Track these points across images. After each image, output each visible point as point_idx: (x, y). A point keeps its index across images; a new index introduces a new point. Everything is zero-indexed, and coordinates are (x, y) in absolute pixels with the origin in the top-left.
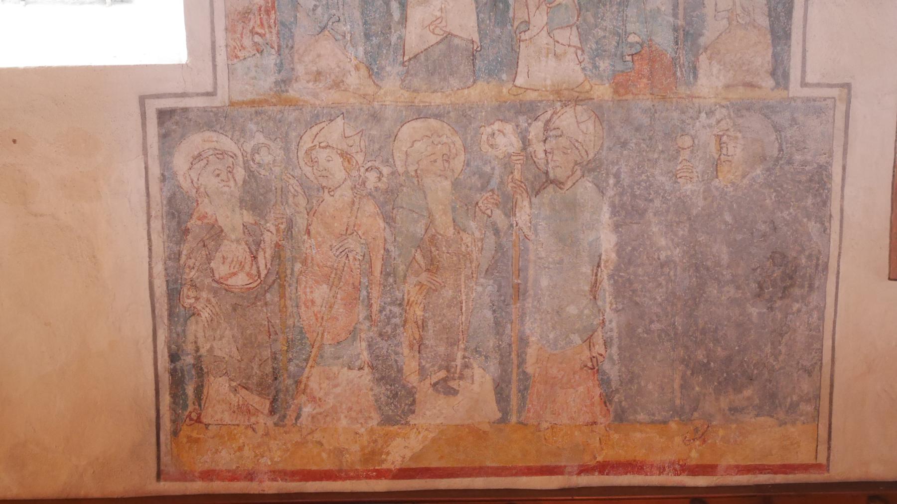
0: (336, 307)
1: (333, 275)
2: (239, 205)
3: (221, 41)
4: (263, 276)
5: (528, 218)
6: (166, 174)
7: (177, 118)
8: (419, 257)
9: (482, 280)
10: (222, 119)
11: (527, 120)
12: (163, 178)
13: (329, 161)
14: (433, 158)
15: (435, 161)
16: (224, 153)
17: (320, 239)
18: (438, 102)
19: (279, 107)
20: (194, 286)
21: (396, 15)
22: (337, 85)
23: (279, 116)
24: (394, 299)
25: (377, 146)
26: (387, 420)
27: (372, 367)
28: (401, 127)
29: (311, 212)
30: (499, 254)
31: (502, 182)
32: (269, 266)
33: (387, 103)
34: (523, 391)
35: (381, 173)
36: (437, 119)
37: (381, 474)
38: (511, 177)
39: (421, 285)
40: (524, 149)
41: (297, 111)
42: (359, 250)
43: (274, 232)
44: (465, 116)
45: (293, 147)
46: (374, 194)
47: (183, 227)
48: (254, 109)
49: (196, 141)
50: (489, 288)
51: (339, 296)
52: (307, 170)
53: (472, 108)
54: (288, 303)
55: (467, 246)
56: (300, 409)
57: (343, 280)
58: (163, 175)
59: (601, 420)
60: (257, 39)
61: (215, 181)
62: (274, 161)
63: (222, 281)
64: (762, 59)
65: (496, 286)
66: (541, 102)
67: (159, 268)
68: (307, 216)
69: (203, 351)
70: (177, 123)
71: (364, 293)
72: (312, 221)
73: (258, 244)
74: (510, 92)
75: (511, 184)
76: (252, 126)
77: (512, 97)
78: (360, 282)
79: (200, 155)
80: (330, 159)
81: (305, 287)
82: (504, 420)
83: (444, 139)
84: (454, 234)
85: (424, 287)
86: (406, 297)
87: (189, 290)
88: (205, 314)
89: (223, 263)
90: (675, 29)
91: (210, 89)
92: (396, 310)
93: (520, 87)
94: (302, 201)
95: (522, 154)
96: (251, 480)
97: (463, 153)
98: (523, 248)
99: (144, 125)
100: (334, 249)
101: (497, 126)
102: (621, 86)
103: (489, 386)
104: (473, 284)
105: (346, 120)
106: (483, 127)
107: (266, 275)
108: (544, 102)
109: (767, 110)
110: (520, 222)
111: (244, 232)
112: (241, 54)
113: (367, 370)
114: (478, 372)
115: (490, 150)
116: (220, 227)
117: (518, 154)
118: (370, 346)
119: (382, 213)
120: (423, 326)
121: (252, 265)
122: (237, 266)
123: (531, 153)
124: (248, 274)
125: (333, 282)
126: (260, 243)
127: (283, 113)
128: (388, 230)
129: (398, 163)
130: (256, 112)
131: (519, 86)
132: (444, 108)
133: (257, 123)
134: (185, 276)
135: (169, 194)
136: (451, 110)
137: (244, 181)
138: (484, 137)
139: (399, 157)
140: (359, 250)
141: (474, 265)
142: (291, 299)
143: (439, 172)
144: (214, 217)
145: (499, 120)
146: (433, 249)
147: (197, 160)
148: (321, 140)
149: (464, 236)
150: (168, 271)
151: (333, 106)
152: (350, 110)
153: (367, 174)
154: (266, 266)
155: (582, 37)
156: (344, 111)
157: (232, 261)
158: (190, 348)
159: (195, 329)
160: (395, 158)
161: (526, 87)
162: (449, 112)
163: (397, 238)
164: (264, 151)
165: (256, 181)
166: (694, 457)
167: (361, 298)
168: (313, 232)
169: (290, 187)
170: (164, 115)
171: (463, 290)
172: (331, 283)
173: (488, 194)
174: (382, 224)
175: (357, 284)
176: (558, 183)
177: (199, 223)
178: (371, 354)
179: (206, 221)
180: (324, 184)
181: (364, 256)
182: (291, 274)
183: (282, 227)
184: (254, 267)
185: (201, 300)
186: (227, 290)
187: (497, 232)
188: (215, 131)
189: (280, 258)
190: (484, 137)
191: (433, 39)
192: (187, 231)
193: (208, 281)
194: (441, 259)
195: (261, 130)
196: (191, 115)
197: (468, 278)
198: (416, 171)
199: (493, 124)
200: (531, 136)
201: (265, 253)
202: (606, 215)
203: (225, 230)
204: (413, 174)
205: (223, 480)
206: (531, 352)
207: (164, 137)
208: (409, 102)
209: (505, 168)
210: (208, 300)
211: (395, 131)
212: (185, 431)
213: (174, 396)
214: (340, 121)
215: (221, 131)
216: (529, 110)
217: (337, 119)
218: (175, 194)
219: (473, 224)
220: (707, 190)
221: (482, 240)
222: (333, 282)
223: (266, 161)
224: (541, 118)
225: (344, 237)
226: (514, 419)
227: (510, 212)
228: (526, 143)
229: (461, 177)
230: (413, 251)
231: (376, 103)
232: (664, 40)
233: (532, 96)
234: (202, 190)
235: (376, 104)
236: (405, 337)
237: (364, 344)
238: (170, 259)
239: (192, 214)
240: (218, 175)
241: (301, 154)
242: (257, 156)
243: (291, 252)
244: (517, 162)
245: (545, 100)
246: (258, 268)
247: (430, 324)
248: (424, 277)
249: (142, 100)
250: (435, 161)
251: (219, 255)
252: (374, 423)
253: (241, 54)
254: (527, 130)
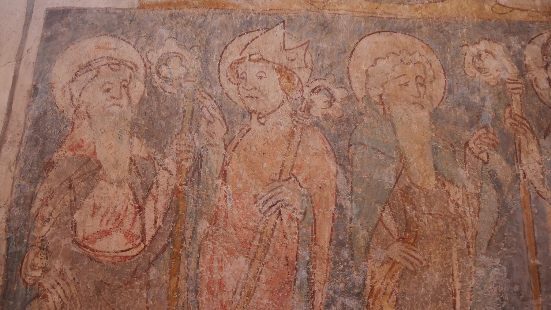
0: (258, 295)
1: (256, 243)
2: (129, 130)
4: (148, 238)
5: (538, 167)
6: (39, 86)
7: (70, 19)
8: (387, 218)
9: (483, 258)
10: (127, 23)
11: (520, 42)
12: (34, 91)
13: (261, 78)
14: (403, 80)
15: (406, 84)
16: (120, 63)
17: (240, 185)
18: (406, 15)
19: (201, 10)
20: (44, 249)
23: (200, 21)
24: (350, 285)
25: (327, 62)
28: (360, 41)
30: (505, 218)
31: (496, 117)
32: (159, 223)
33: (340, 12)
35: (332, 96)
36: (405, 34)
38: (508, 110)
39: (391, 262)
40: (522, 75)
41: (223, 15)
42: (297, 204)
43: (174, 172)
44: (442, 32)
45: (214, 58)
46: (323, 123)
47: (46, 160)
48: (169, 11)
50: (495, 271)
51: (263, 276)
52: (231, 88)
53: (449, 23)
54: (183, 284)
55: (457, 204)
57: (271, 250)
58: (35, 87)
61: (102, 97)
62: (187, 74)
63: (86, 243)
65: (505, 268)
66: (533, 22)
68: (224, 151)
70: (68, 25)
72: (231, 158)
73: (148, 188)
74: (494, 9)
75: (509, 121)
76: (163, 32)
77: (498, 16)
78: (297, 255)
79: (89, 64)
80: (263, 75)
81: (212, 259)
83: (417, 58)
84: (437, 187)
85: (397, 266)
86: (368, 282)
87: (36, 255)
89: (92, 215)
93: (504, 6)
94: (219, 129)
95: (520, 81)
97: (443, 76)
98: (536, 211)
99: (27, 25)
100: (261, 202)
101: (483, 46)
104: (471, 264)
105: (287, 30)
106: (466, 47)
107: (153, 237)
108: (537, 23)
110: (528, 172)
111: (130, 169)
115: (478, 74)
116: (98, 162)
117: (515, 82)
119: (333, 150)
121: (135, 219)
122: (113, 220)
123: (531, 80)
124: (128, 235)
125: (255, 254)
126: (152, 186)
127: (206, 17)
128: (341, 176)
129: (356, 85)
130: (171, 15)
131: (503, 4)
132: (414, 23)
133: (171, 28)
134: (34, 233)
135: (37, 113)
136: (422, 24)
137: (142, 99)
138: (469, 59)
139: (355, 74)
140: (297, 204)
141: (469, 234)
142: (187, 278)
143: (412, 99)
144: (92, 147)
145: (486, 39)
146: (408, 208)
147: (84, 70)
148: (253, 51)
149: (453, 190)
150: (11, 223)
151: (271, 12)
152: (294, 17)
153: (314, 96)
154: (156, 222)
156: (285, 19)
157: (106, 213)
160: (353, 79)
161: (511, 6)
162: (420, 27)
163: (355, 189)
164: (174, 62)
165: (158, 100)
167: (298, 282)
168: (231, 174)
169: (205, 110)
171: (456, 273)
172: (252, 256)
173: (481, 132)
174: (333, 168)
175: (292, 258)
177: (70, 154)
179: (79, 152)
180: (252, 108)
181: (305, 214)
182: (192, 238)
183: (187, 164)
184: (138, 224)
185: (51, 273)
186: (90, 258)
187: (498, 185)
188: (115, 36)
189: (177, 212)
190: (469, 59)
192: (51, 165)
193: (66, 241)
194: (421, 223)
195: (175, 37)
196: (88, 17)
197: (463, 253)
198: (380, 96)
199: (478, 43)
200: (528, 60)
201: (156, 202)
203: (104, 166)
204: (377, 99)
207: (47, 40)
208: (369, 13)
209: (500, 99)
210: (62, 274)
211: (352, 46)
214: (279, 30)
215: (122, 37)
217: (276, 28)
218: (45, 113)
219: (463, 173)
221: (478, 196)
222: (255, 254)
223: (175, 75)
224: (536, 40)
225: (276, 184)
229: (443, 107)
230: (379, 209)
231: (327, 11)
234: (83, 109)
235: (327, 13)
238: (18, 205)
239: (62, 142)
240: (108, 90)
241: (224, 67)
242: (164, 68)
243: (196, 202)
244: (516, 91)
245: (537, 21)
246: (143, 225)
248: (396, 250)
250: (406, 84)
251: (89, 202)
254: (520, 53)
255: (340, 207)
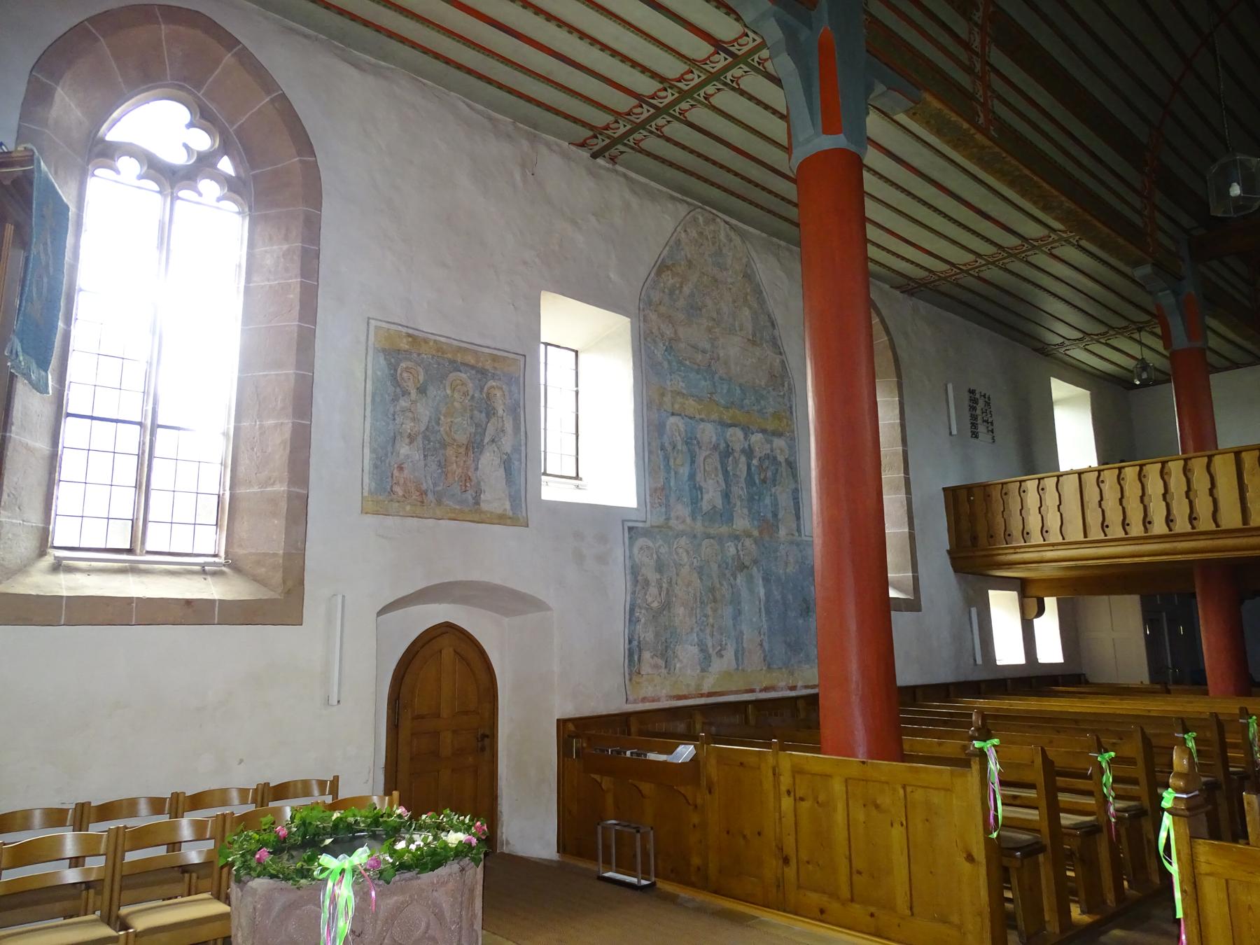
3: (648, 501)
12: (630, 557)
18: (712, 532)
20: (640, 608)
21: (700, 497)
22: (684, 522)
26: (703, 670)
27: (698, 645)
29: (677, 575)
34: (743, 654)
37: (702, 695)
40: (737, 552)
49: (641, 542)
56: (675, 666)
59: (764, 668)
60: (660, 501)
64: (794, 526)
67: (628, 598)
69: (641, 639)
71: (694, 611)
82: (737, 669)
88: (643, 620)
90: (772, 512)
91: (644, 519)
92: (705, 619)
96: (659, 701)
102: (761, 533)
103: (733, 653)
109: (798, 545)
112: (655, 506)
113: (696, 646)
114: (729, 645)
118: (697, 635)
120: (713, 626)
124: (659, 602)
129: (703, 556)
137: (657, 561)
155: (750, 511)
158: (636, 637)
159: (639, 627)
164: (662, 547)
166: (791, 683)
170: (630, 529)
176: (748, 568)
178: (698, 638)
191: (710, 508)
192: (637, 581)
193: (645, 605)
202: (761, 582)
205: (650, 702)
206: (745, 637)
207: (630, 538)
212: (635, 678)
213: (629, 661)
214: (684, 537)
216: (737, 538)
220: (785, 573)
226: (740, 668)
227: (735, 579)
228: (738, 551)
232: (769, 516)
233: (738, 532)
236: (708, 631)
237: (695, 635)
247: (715, 626)
249: (623, 521)
252: (698, 671)
253: (655, 506)
255: (701, 593)
